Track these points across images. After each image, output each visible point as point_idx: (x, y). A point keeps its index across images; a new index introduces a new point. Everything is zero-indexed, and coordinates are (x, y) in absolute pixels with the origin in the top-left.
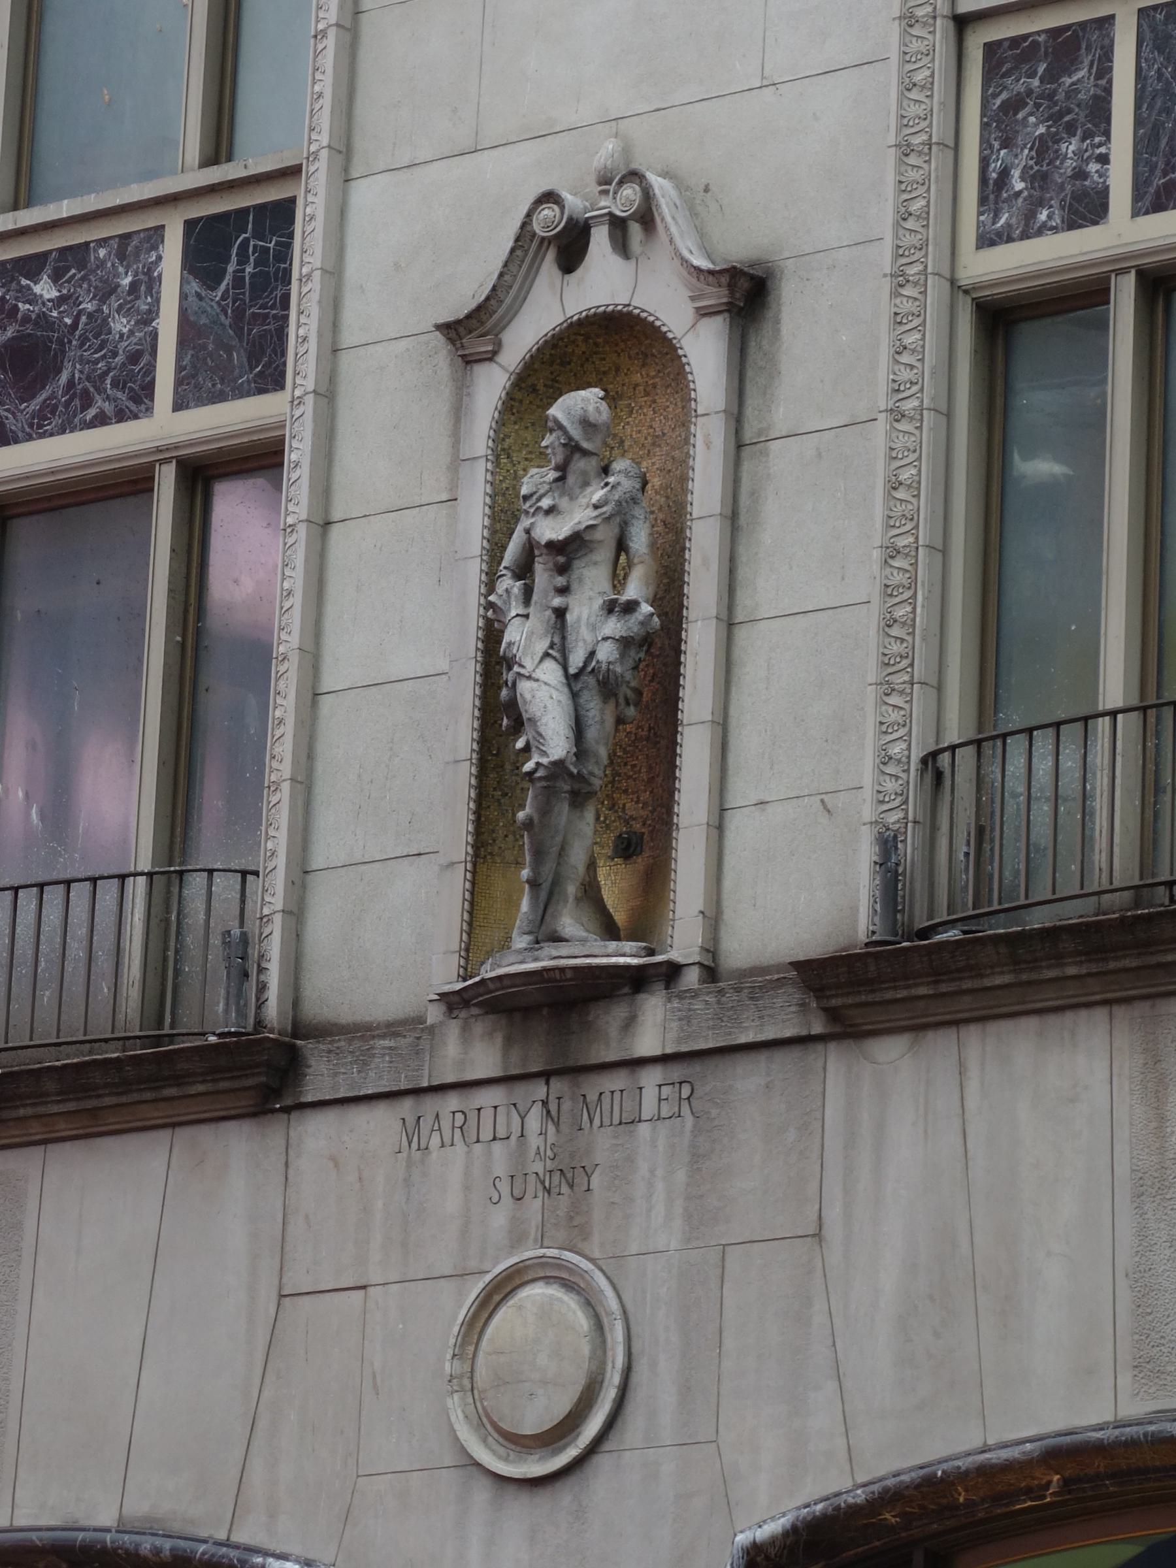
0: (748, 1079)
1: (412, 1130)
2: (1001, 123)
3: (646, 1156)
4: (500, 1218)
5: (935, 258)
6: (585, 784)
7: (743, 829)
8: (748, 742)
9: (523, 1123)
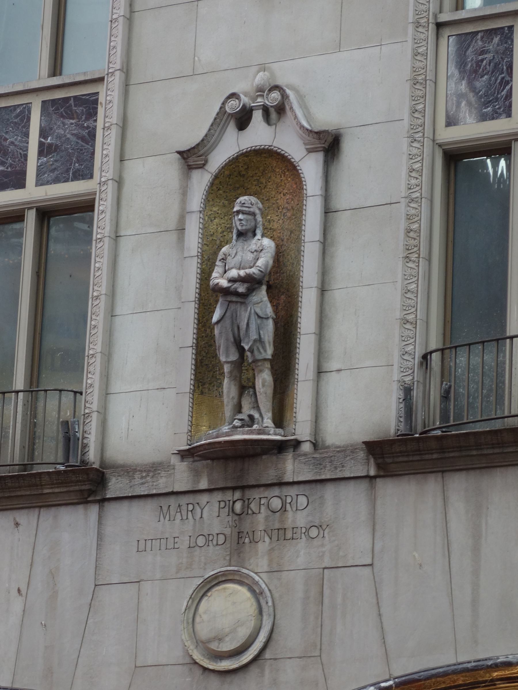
5: (428, 132)
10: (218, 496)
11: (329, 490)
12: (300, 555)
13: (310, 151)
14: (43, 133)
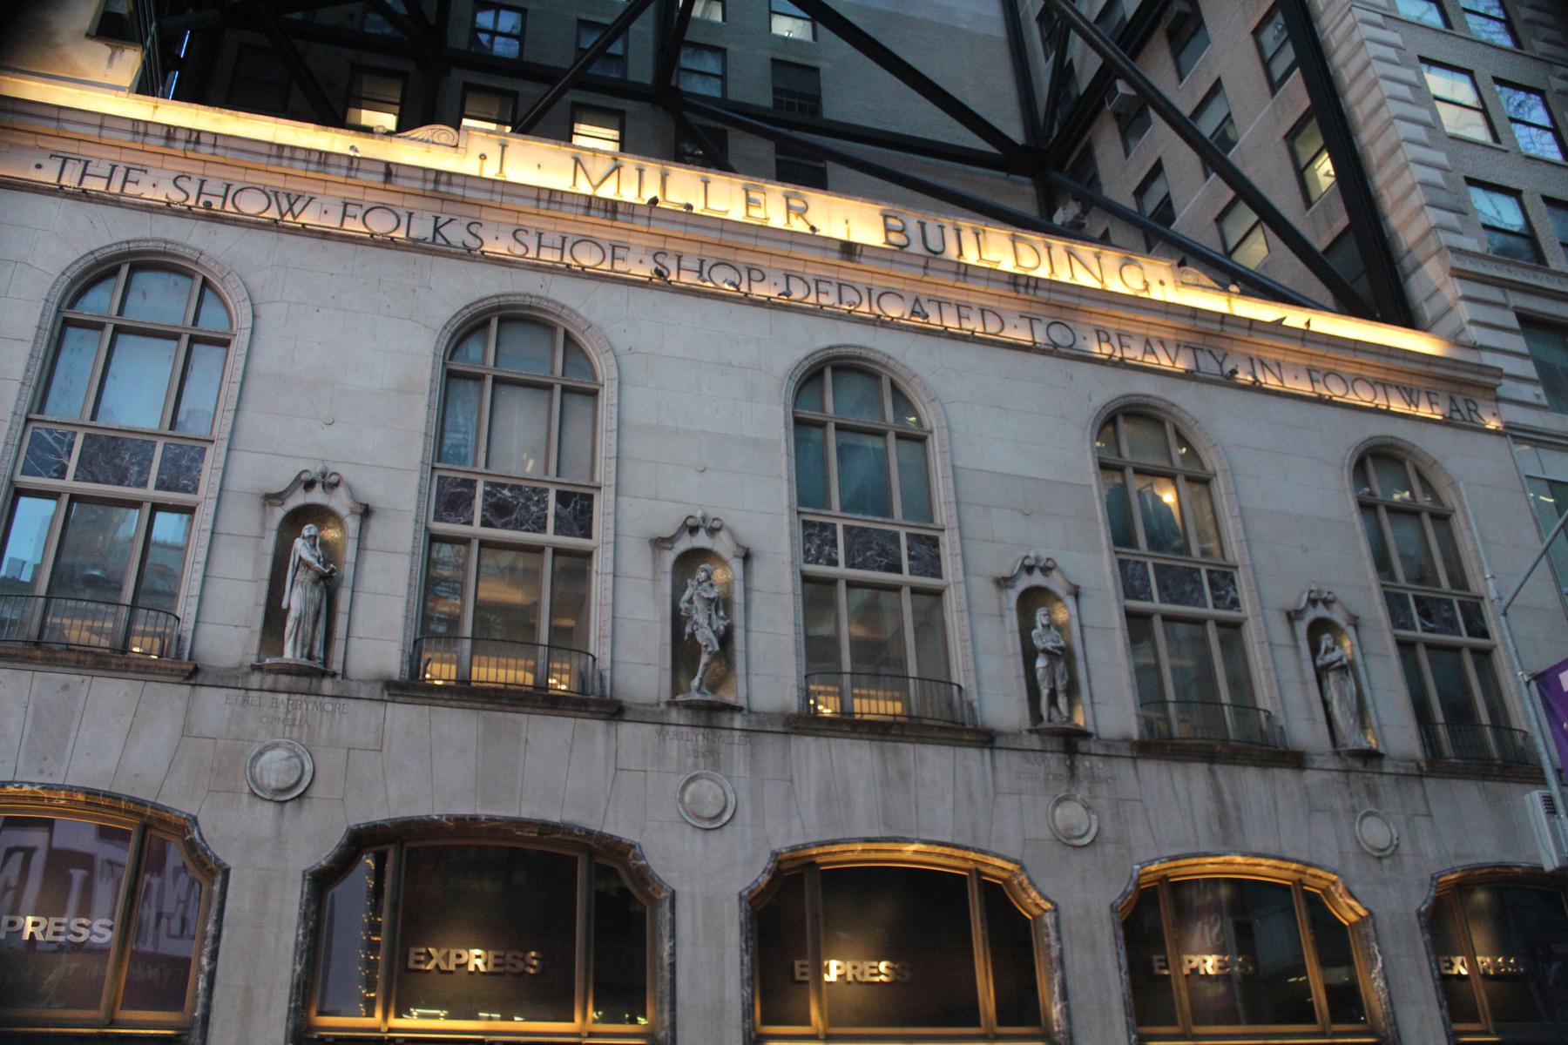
0: (768, 739)
1: (661, 733)
2: (808, 538)
3: (736, 750)
4: (690, 761)
6: (700, 656)
7: (754, 680)
8: (753, 660)
9: (699, 738)
10: (1055, 756)
11: (1114, 761)
12: (1103, 791)
14: (909, 549)
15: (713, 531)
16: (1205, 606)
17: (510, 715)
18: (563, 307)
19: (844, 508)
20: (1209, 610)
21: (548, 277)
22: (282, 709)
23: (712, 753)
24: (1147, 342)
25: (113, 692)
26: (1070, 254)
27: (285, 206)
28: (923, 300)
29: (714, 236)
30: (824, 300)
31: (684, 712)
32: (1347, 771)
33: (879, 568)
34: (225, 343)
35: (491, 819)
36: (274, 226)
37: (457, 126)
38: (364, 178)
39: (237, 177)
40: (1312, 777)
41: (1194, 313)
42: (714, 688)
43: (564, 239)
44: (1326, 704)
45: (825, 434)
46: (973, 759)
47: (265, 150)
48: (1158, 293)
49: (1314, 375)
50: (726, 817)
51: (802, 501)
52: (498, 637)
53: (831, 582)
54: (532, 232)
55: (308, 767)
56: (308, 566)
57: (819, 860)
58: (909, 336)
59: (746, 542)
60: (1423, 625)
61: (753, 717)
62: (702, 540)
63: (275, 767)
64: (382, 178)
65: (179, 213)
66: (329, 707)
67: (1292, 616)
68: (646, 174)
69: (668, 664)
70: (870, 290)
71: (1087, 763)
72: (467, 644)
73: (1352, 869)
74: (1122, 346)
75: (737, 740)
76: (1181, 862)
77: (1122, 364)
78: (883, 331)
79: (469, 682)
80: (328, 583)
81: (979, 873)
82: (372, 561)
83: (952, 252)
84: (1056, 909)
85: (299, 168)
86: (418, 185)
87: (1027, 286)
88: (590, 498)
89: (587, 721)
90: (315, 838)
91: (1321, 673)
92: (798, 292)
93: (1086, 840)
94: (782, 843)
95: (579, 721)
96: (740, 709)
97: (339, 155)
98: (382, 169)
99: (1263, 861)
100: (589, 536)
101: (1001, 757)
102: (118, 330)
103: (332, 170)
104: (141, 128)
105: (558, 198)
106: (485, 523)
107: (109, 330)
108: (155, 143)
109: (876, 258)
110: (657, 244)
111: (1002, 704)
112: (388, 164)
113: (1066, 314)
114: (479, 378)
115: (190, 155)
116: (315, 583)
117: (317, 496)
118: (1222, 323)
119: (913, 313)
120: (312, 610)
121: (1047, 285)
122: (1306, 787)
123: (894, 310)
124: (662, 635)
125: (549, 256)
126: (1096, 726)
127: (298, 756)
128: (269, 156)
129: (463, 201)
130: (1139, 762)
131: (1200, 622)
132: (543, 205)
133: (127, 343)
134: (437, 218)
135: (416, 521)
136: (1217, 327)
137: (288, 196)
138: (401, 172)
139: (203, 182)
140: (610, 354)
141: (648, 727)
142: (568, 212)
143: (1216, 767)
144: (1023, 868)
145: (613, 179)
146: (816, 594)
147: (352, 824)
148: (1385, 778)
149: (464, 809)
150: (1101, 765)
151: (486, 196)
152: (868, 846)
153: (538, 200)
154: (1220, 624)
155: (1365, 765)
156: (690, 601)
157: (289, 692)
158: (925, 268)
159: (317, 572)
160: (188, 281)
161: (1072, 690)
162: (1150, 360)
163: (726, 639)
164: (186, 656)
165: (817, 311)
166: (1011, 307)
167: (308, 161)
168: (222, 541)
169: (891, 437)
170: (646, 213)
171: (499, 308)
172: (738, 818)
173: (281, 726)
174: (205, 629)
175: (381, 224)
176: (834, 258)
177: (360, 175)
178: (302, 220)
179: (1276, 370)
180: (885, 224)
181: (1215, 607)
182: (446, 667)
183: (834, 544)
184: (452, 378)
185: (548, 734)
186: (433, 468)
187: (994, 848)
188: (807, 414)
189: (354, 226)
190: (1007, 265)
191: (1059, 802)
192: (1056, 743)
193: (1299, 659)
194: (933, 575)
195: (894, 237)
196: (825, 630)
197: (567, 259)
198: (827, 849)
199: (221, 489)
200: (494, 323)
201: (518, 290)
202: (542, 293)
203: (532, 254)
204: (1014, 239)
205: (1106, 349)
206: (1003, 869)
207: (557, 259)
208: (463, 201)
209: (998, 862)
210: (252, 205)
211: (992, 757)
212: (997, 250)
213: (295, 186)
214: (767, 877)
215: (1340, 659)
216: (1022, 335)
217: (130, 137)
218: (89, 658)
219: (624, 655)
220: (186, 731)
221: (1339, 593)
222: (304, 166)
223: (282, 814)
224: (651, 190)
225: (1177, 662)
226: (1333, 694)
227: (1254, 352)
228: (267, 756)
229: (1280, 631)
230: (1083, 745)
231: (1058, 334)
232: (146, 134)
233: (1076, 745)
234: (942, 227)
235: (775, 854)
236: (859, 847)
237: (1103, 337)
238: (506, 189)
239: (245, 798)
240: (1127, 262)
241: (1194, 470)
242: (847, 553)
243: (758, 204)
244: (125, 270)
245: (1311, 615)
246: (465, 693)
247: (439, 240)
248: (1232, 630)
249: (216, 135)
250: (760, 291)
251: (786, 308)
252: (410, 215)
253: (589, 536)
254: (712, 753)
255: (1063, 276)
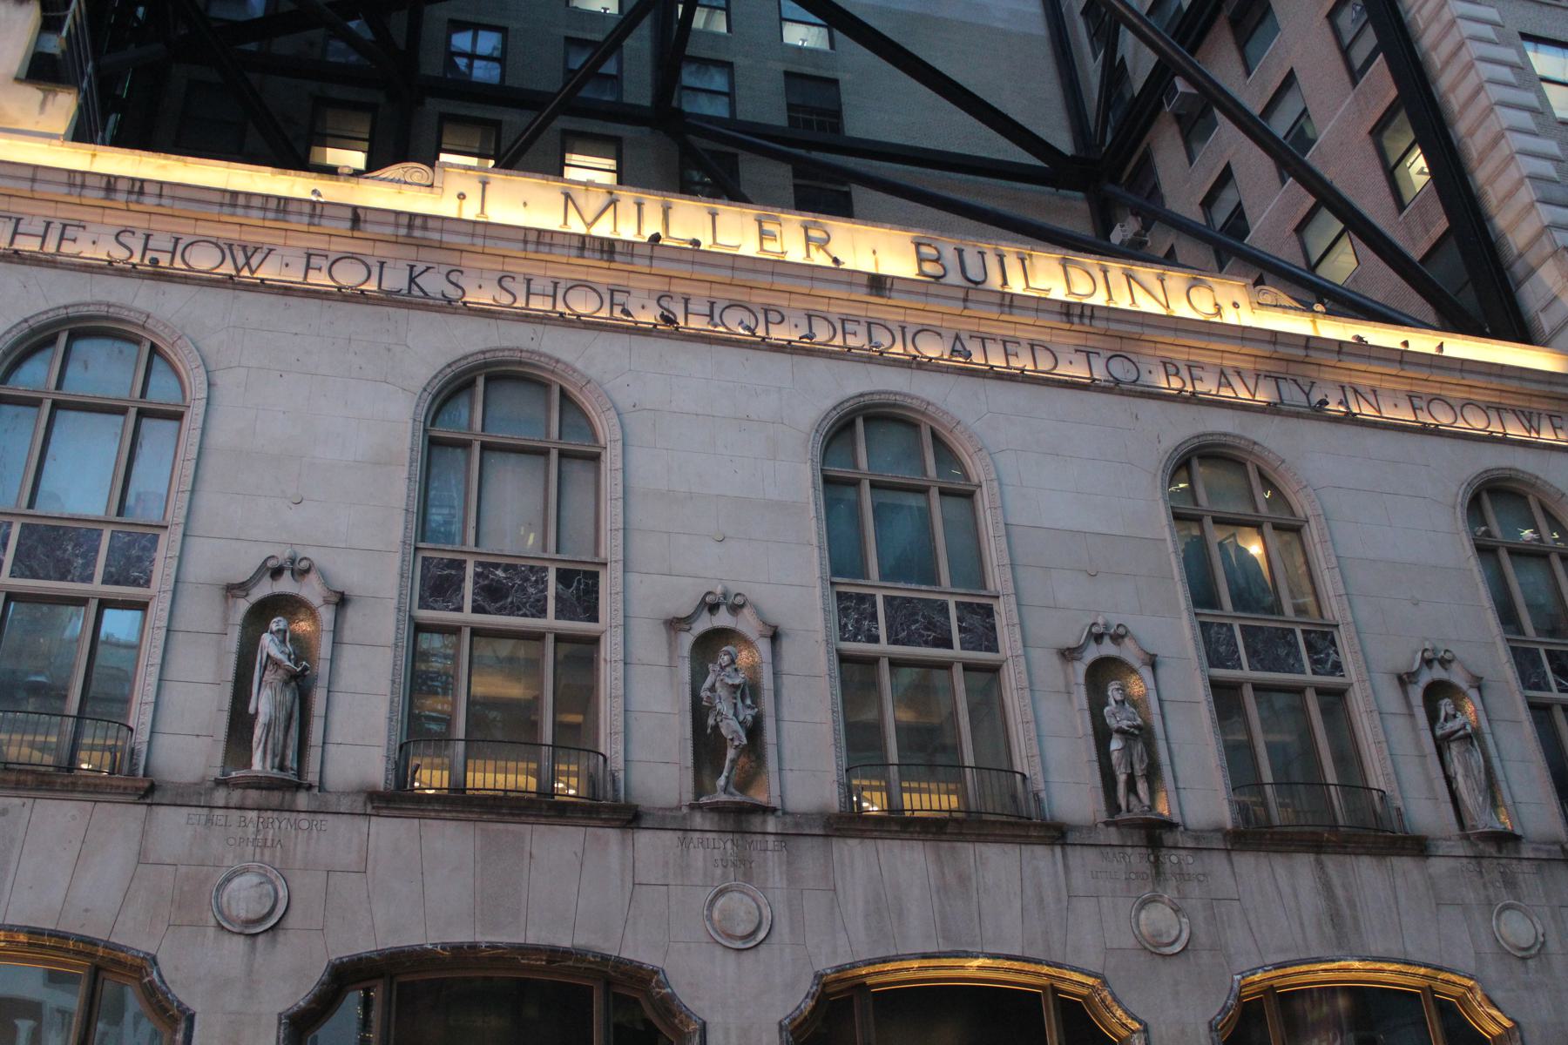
0: (806, 843)
1: (682, 841)
2: (843, 612)
4: (719, 871)
6: (726, 751)
8: (786, 753)
9: (727, 846)
12: (1194, 890)
13: (762, 636)
14: (960, 620)
15: (735, 609)
16: (1303, 672)
17: (512, 827)
18: (558, 361)
19: (883, 577)
20: (1308, 677)
21: (539, 328)
22: (251, 829)
23: (744, 865)
24: (1222, 373)
25: (57, 817)
26: (1129, 277)
27: (241, 260)
28: (964, 336)
29: (724, 275)
30: (852, 341)
31: (710, 815)
32: (1478, 857)
33: (927, 644)
34: (177, 416)
35: (493, 946)
36: (229, 282)
37: (431, 161)
38: (328, 225)
39: (186, 229)
40: (1437, 866)
41: (1274, 337)
42: (743, 786)
43: (556, 285)
44: (1449, 780)
45: (859, 494)
46: (1042, 858)
47: (217, 198)
48: (1230, 317)
49: (1417, 402)
50: (761, 935)
51: (836, 571)
52: (499, 736)
53: (871, 662)
54: (520, 278)
55: (283, 893)
56: (277, 664)
57: (869, 981)
58: (951, 378)
59: (774, 620)
60: (1559, 684)
61: (788, 819)
62: (723, 619)
63: (244, 897)
64: (349, 224)
65: (122, 273)
66: (305, 825)
67: (1404, 680)
68: (646, 209)
69: (689, 761)
70: (903, 329)
71: (1174, 859)
72: (460, 747)
73: (1492, 972)
74: (1192, 380)
75: (770, 845)
76: (1289, 970)
77: (1194, 399)
78: (920, 375)
79: (464, 790)
80: (300, 683)
81: (1055, 990)
82: (349, 655)
83: (995, 281)
84: (1146, 1030)
85: (255, 217)
86: (389, 230)
87: (1082, 316)
88: (595, 575)
89: (600, 831)
90: (291, 977)
91: (1441, 745)
92: (822, 334)
93: (1177, 948)
94: (826, 962)
95: (590, 830)
96: (774, 810)
97: (300, 200)
98: (349, 214)
99: (1385, 966)
100: (594, 618)
101: (1075, 855)
102: (57, 405)
103: (293, 218)
104: (78, 180)
105: (547, 240)
106: (477, 609)
107: (47, 405)
108: (94, 197)
109: (909, 292)
110: (659, 285)
111: (1073, 793)
112: (355, 209)
113: (1128, 346)
114: (466, 445)
115: (132, 206)
116: (286, 683)
117: (285, 585)
118: (1307, 347)
119: (953, 351)
120: (282, 716)
121: (1105, 314)
122: (1430, 877)
123: (932, 349)
124: (683, 727)
125: (539, 304)
126: (1181, 814)
127: (271, 882)
128: (222, 205)
129: (441, 247)
130: (1236, 857)
131: (1298, 690)
132: (531, 247)
133: (66, 419)
134: (412, 267)
135: (399, 610)
136: (1301, 352)
137: (244, 248)
138: (370, 217)
139: (148, 237)
140: (612, 413)
141: (670, 833)
142: (558, 255)
143: (1324, 857)
144: (1105, 983)
145: (609, 213)
146: (856, 674)
147: (333, 957)
148: (1525, 863)
149: (462, 936)
150: (1190, 860)
151: (467, 240)
152: (926, 963)
153: (525, 242)
154: (1321, 692)
155: (1500, 850)
156: (712, 689)
157: (259, 809)
158: (965, 300)
159: (288, 671)
160: (133, 349)
161: (1153, 773)
162: (1226, 392)
163: (754, 731)
164: (141, 772)
165: (846, 354)
166: (1065, 339)
167: (264, 209)
168: (178, 638)
169: (934, 493)
170: (647, 251)
171: (486, 365)
172: (775, 938)
173: (250, 848)
174: (162, 741)
175: (349, 276)
176: (861, 294)
177: (324, 222)
178: (260, 274)
179: (1372, 399)
180: (918, 252)
181: (1314, 672)
182: (437, 773)
183: (874, 617)
184: (434, 445)
185: (554, 845)
186: (416, 549)
187: (1070, 960)
188: (836, 471)
189: (319, 279)
190: (1059, 293)
191: (1144, 904)
192: (1137, 836)
193: (1414, 728)
194: (988, 649)
195: (929, 268)
196: (869, 716)
197: (561, 308)
198: (878, 967)
199: (177, 581)
200: (481, 382)
201: (506, 344)
202: (533, 346)
203: (521, 303)
204: (1065, 263)
205: (1176, 383)
206: (1083, 984)
207: (549, 308)
208: (441, 247)
209: (1077, 977)
210: (204, 260)
211: (1064, 856)
212: (1047, 277)
213: (251, 237)
214: (810, 1003)
215: (1464, 727)
216: (1076, 370)
217: (65, 190)
218: (30, 778)
219: (636, 755)
220: (142, 857)
221: (1457, 650)
222: (260, 214)
223: (253, 949)
224: (652, 226)
225: (1276, 738)
226: (1457, 768)
227: (1345, 379)
228: (236, 883)
229: (1391, 696)
230: (1168, 838)
231: (1120, 369)
232: (83, 186)
233: (1161, 839)
234: (982, 254)
235: (818, 976)
236: (916, 964)
237: (1171, 369)
238: (490, 232)
239: (211, 932)
240: (1195, 283)
241: (1284, 517)
242: (889, 628)
243: (773, 237)
244: (63, 338)
245: (1426, 677)
246: (460, 802)
247: (416, 291)
248: (1334, 699)
249: (161, 183)
250: (779, 334)
251: (809, 352)
252: (382, 264)
253: (596, 620)
254: (744, 865)
255: (1122, 302)
